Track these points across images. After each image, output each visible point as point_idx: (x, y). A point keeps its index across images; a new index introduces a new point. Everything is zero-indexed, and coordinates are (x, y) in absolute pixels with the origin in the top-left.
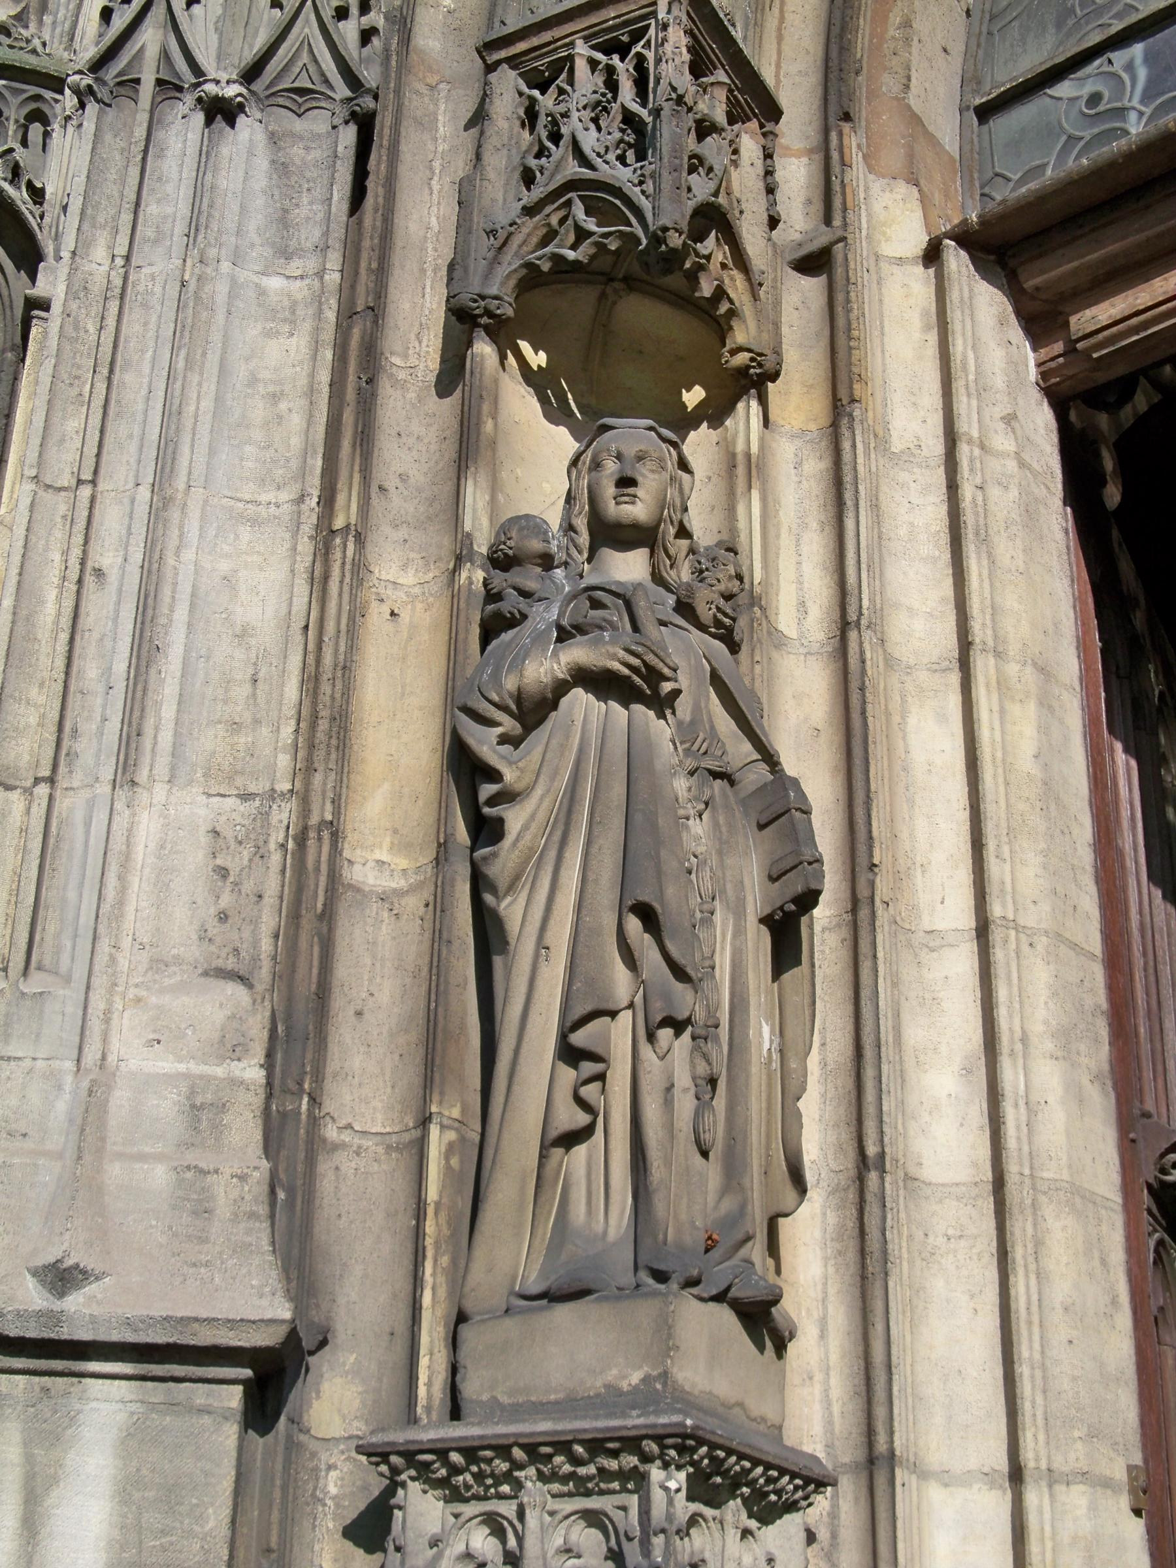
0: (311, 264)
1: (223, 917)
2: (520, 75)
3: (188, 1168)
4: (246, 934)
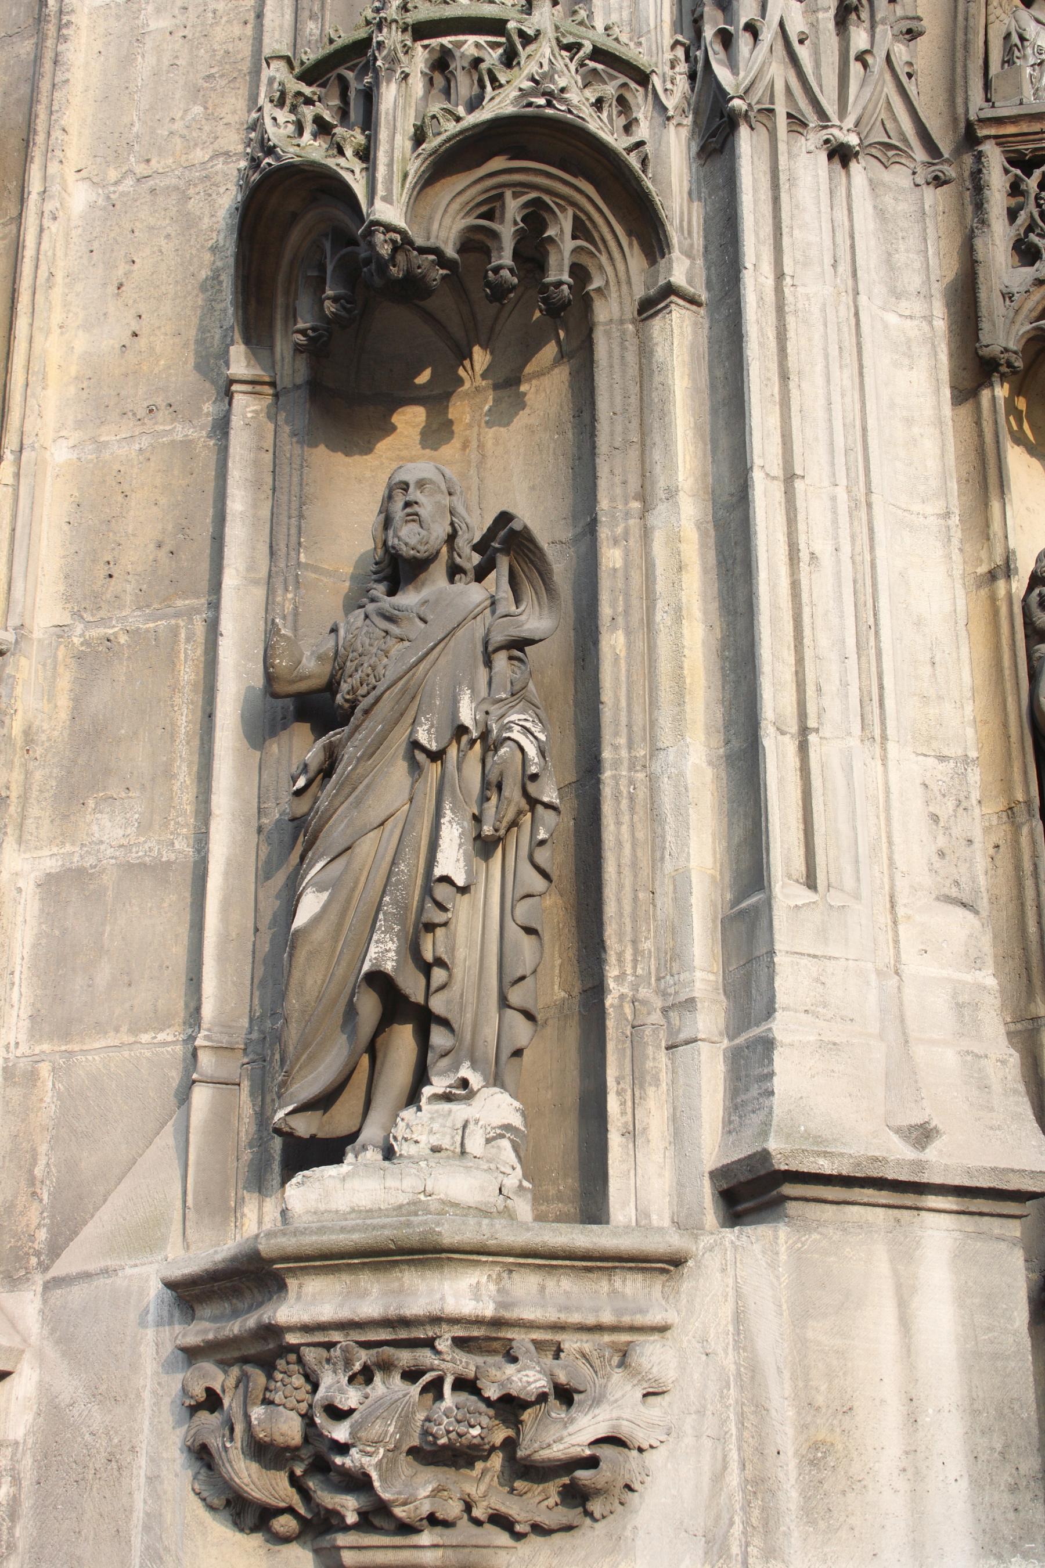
0: (917, 307)
1: (941, 854)
2: (1003, 152)
3: (967, 1052)
4: (963, 868)
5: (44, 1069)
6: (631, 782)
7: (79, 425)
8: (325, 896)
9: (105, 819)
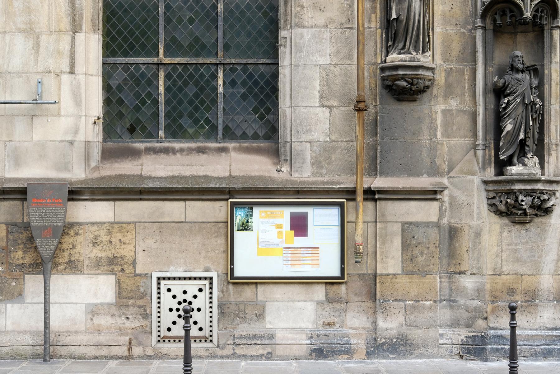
5: (445, 143)
6: (548, 109)
7: (442, 24)
8: (512, 126)
9: (453, 101)
